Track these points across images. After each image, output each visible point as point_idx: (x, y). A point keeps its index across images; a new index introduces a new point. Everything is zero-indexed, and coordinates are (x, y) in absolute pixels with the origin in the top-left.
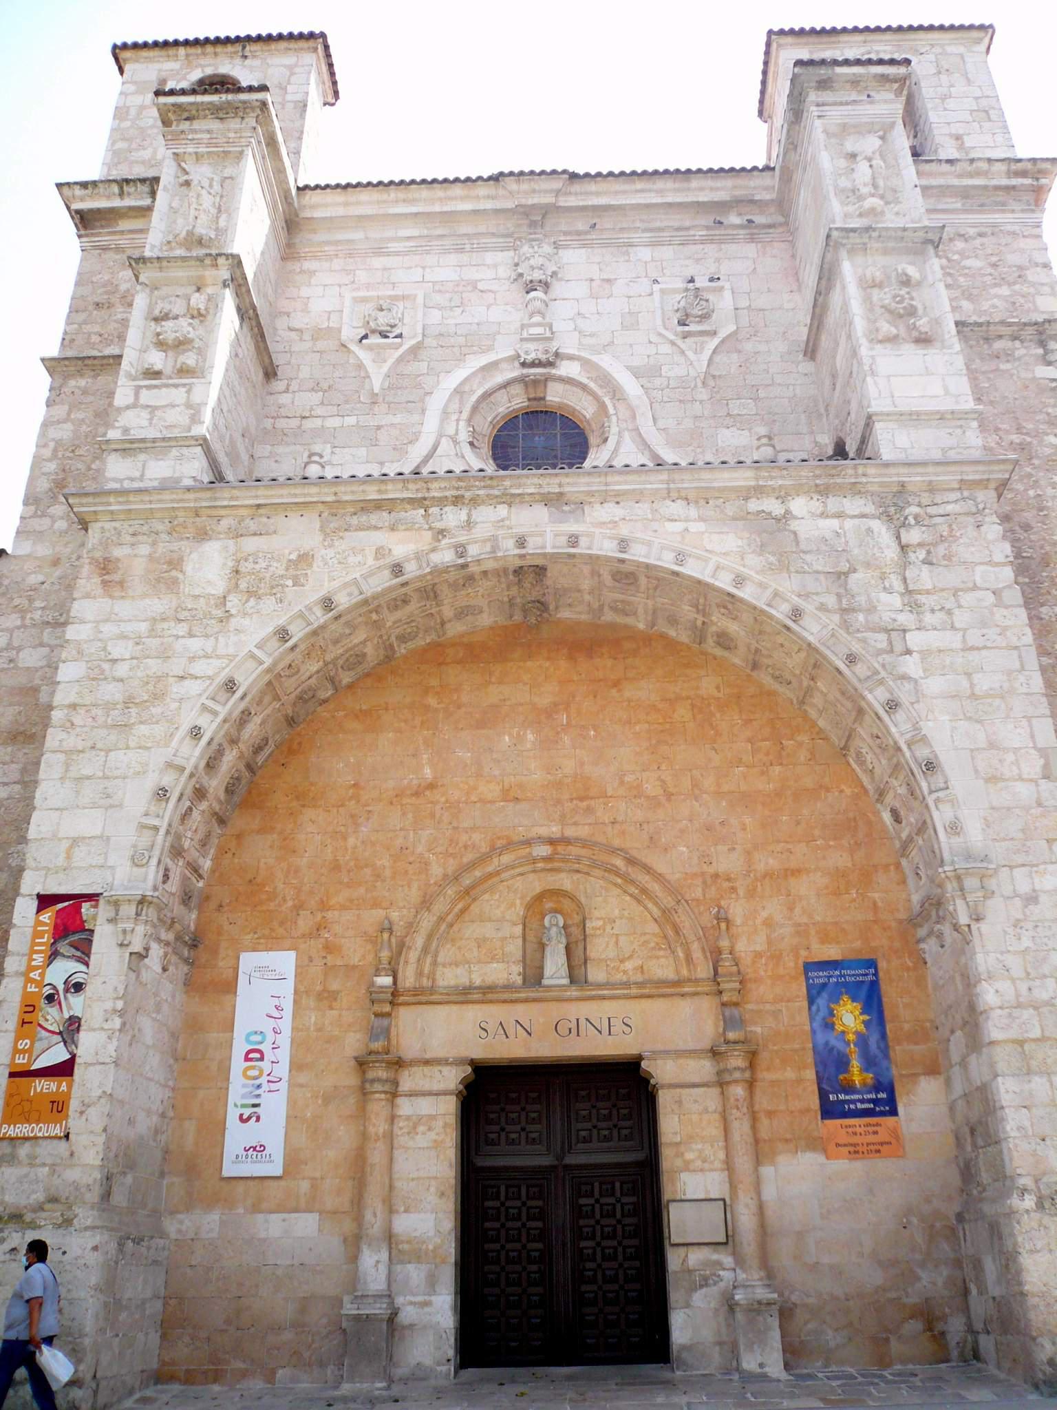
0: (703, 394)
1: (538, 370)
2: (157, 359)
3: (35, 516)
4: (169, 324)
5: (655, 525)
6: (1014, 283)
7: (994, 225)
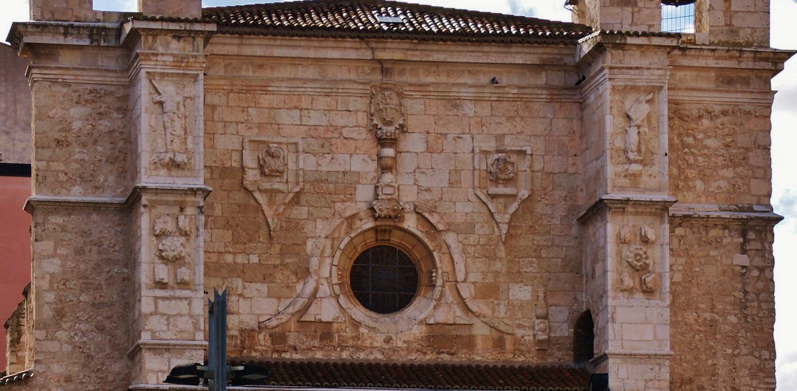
1: (388, 221)
2: (163, 273)
3: (46, 339)
6: (739, 165)
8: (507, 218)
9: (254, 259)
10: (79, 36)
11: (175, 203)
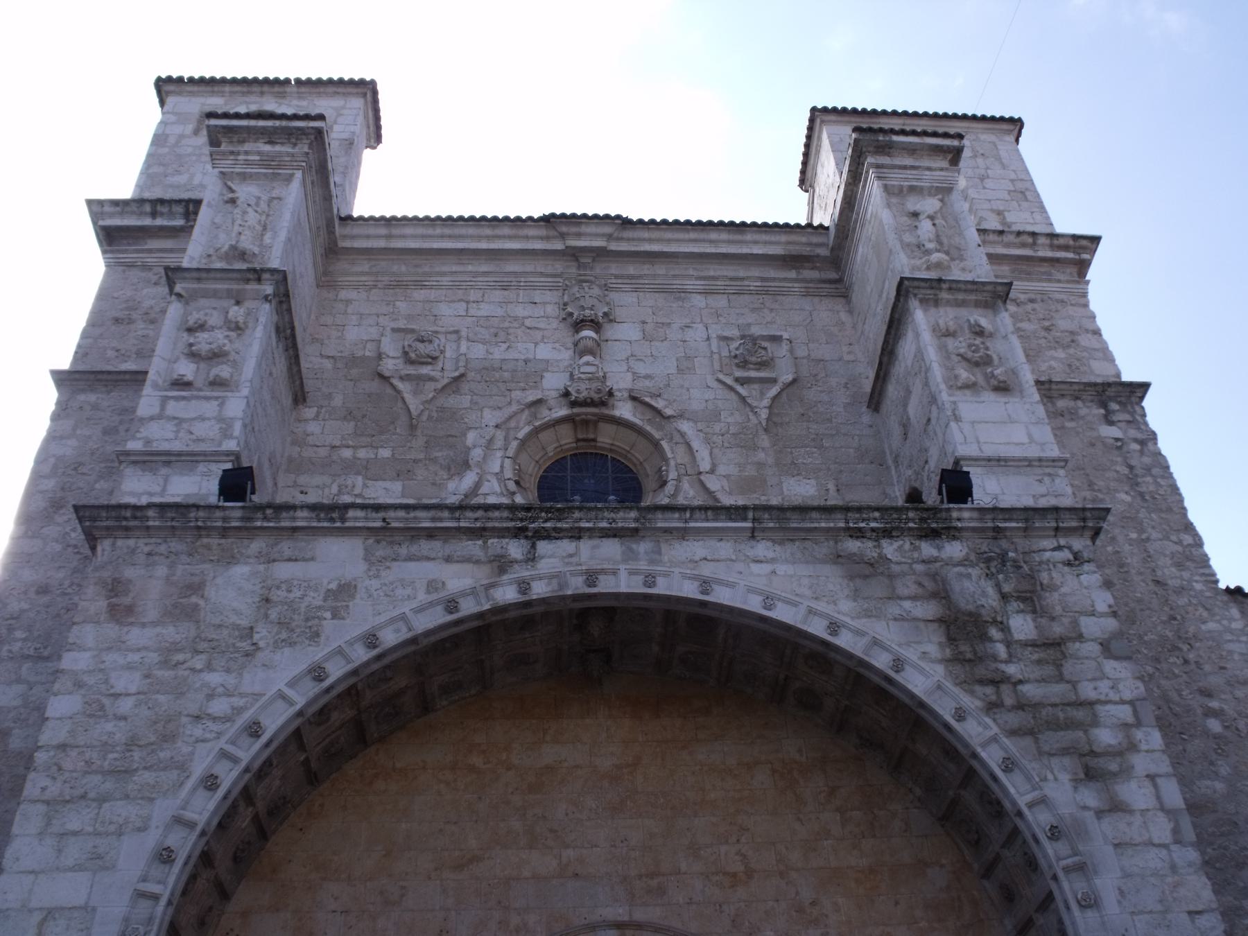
0: (765, 441)
1: (589, 409)
2: (186, 369)
4: (202, 336)
5: (740, 566)
6: (1069, 347)
7: (1042, 293)
8: (766, 402)
9: (385, 453)
10: (171, 215)
11: (229, 294)
